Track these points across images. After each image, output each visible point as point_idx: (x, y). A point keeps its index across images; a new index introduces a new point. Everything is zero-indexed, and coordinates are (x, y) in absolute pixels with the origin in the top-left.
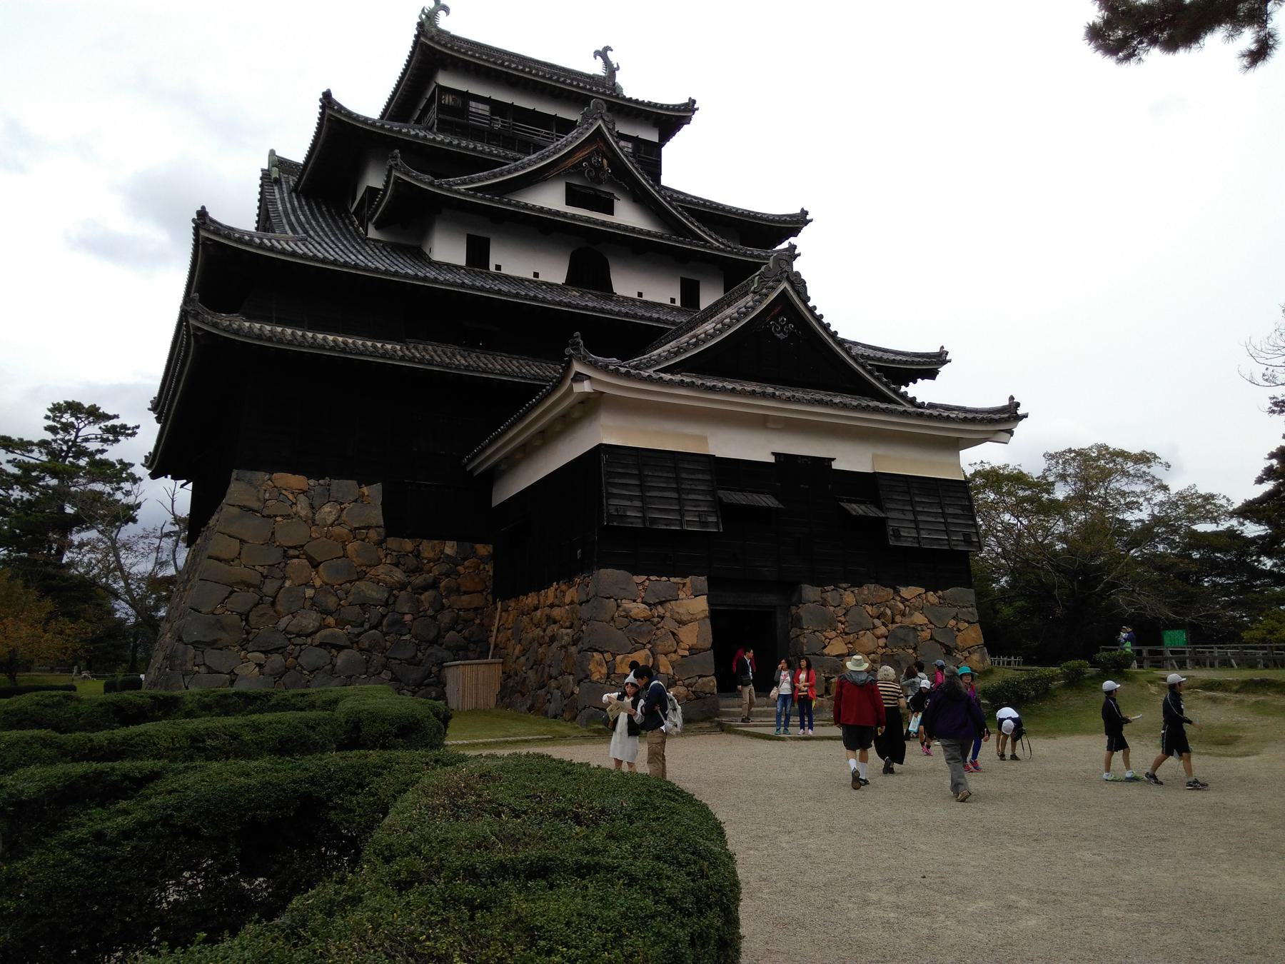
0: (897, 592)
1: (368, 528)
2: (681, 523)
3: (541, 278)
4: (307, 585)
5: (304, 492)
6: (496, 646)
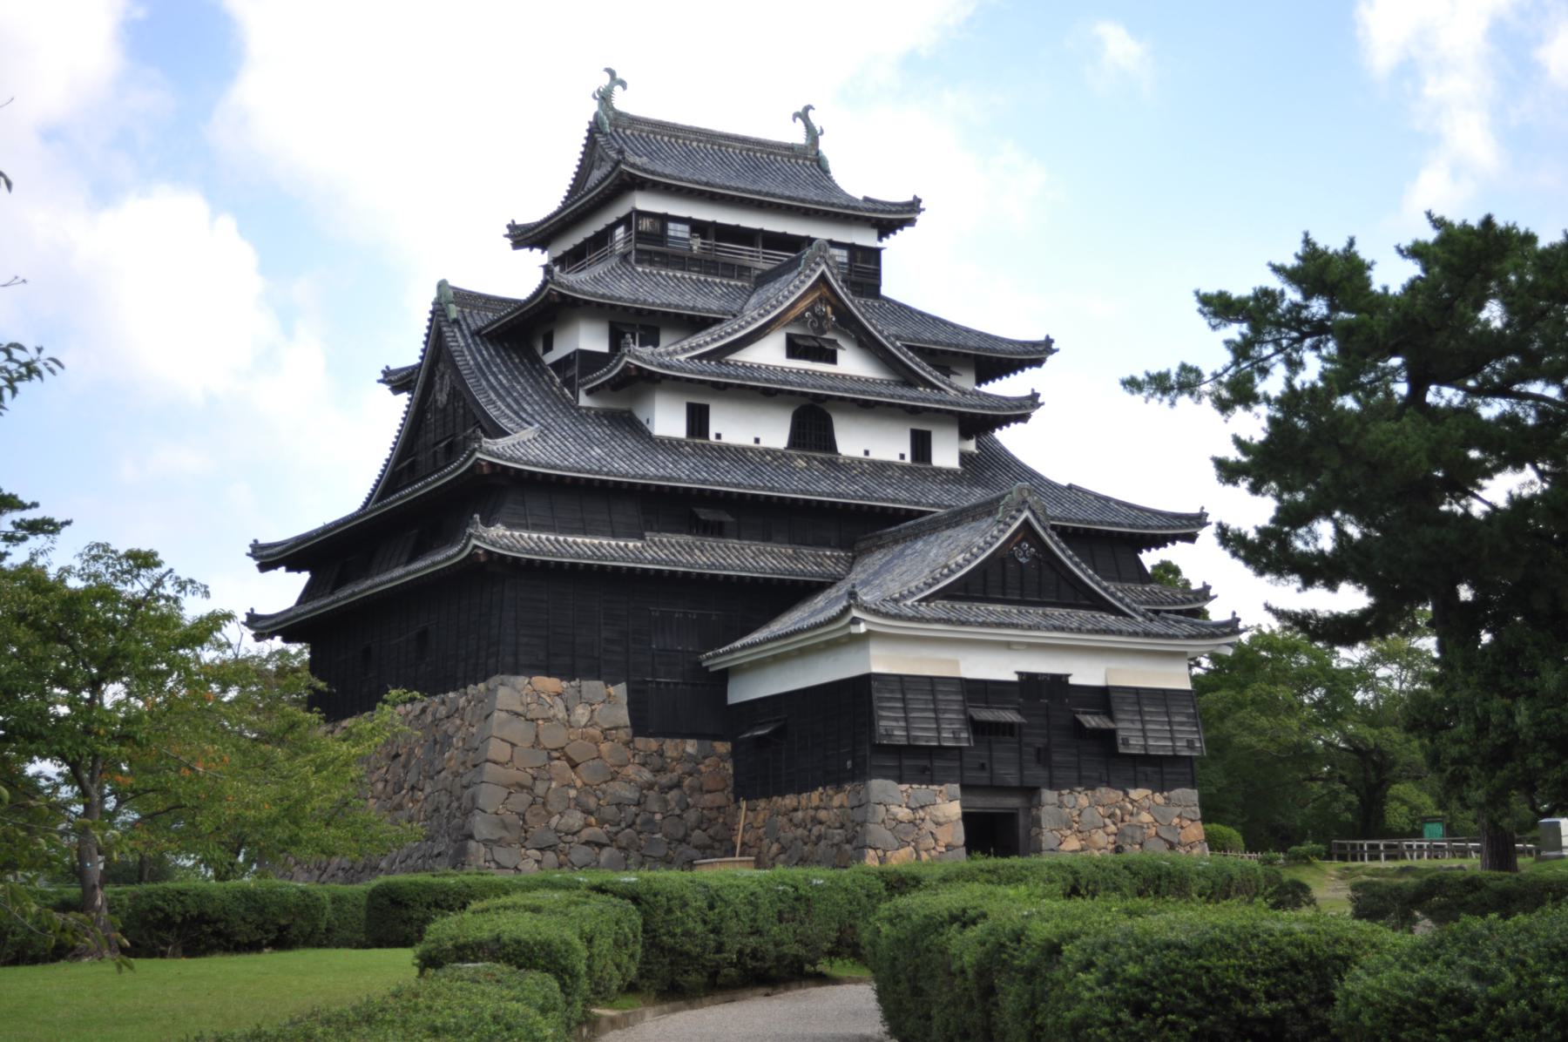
0: (1126, 794)
1: (616, 728)
2: (939, 739)
3: (764, 444)
4: (569, 786)
5: (559, 694)
6: (743, 844)
